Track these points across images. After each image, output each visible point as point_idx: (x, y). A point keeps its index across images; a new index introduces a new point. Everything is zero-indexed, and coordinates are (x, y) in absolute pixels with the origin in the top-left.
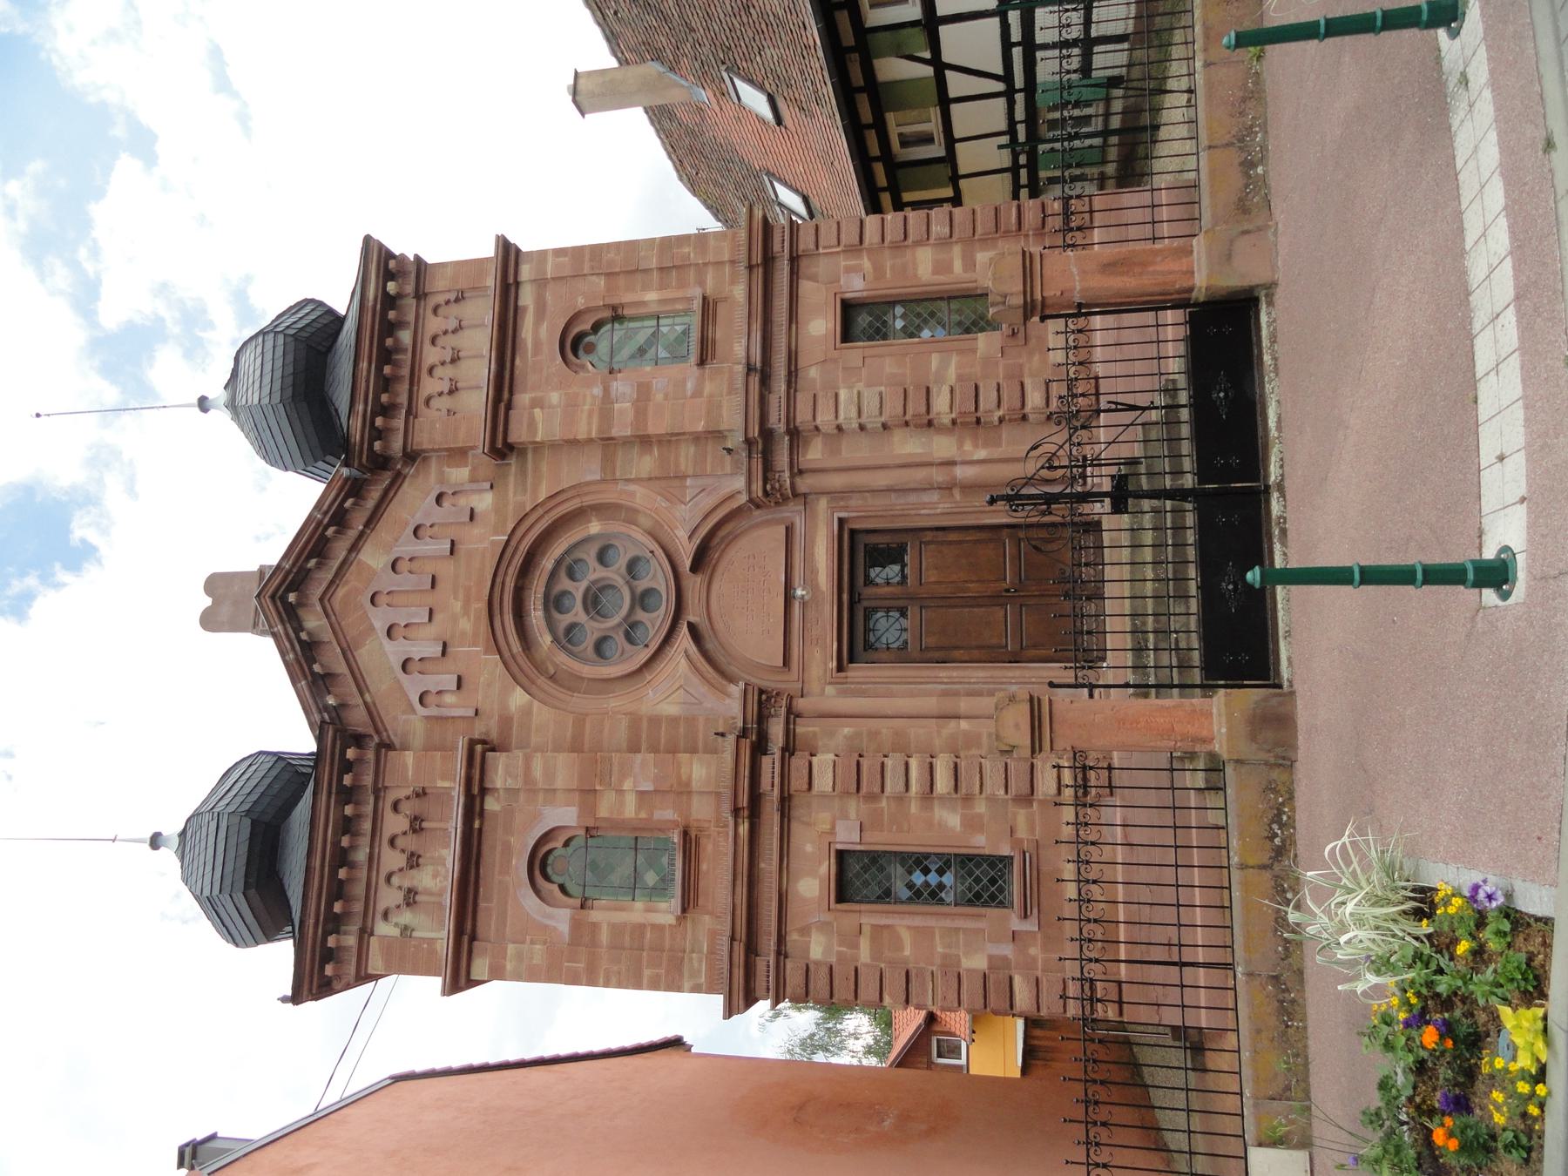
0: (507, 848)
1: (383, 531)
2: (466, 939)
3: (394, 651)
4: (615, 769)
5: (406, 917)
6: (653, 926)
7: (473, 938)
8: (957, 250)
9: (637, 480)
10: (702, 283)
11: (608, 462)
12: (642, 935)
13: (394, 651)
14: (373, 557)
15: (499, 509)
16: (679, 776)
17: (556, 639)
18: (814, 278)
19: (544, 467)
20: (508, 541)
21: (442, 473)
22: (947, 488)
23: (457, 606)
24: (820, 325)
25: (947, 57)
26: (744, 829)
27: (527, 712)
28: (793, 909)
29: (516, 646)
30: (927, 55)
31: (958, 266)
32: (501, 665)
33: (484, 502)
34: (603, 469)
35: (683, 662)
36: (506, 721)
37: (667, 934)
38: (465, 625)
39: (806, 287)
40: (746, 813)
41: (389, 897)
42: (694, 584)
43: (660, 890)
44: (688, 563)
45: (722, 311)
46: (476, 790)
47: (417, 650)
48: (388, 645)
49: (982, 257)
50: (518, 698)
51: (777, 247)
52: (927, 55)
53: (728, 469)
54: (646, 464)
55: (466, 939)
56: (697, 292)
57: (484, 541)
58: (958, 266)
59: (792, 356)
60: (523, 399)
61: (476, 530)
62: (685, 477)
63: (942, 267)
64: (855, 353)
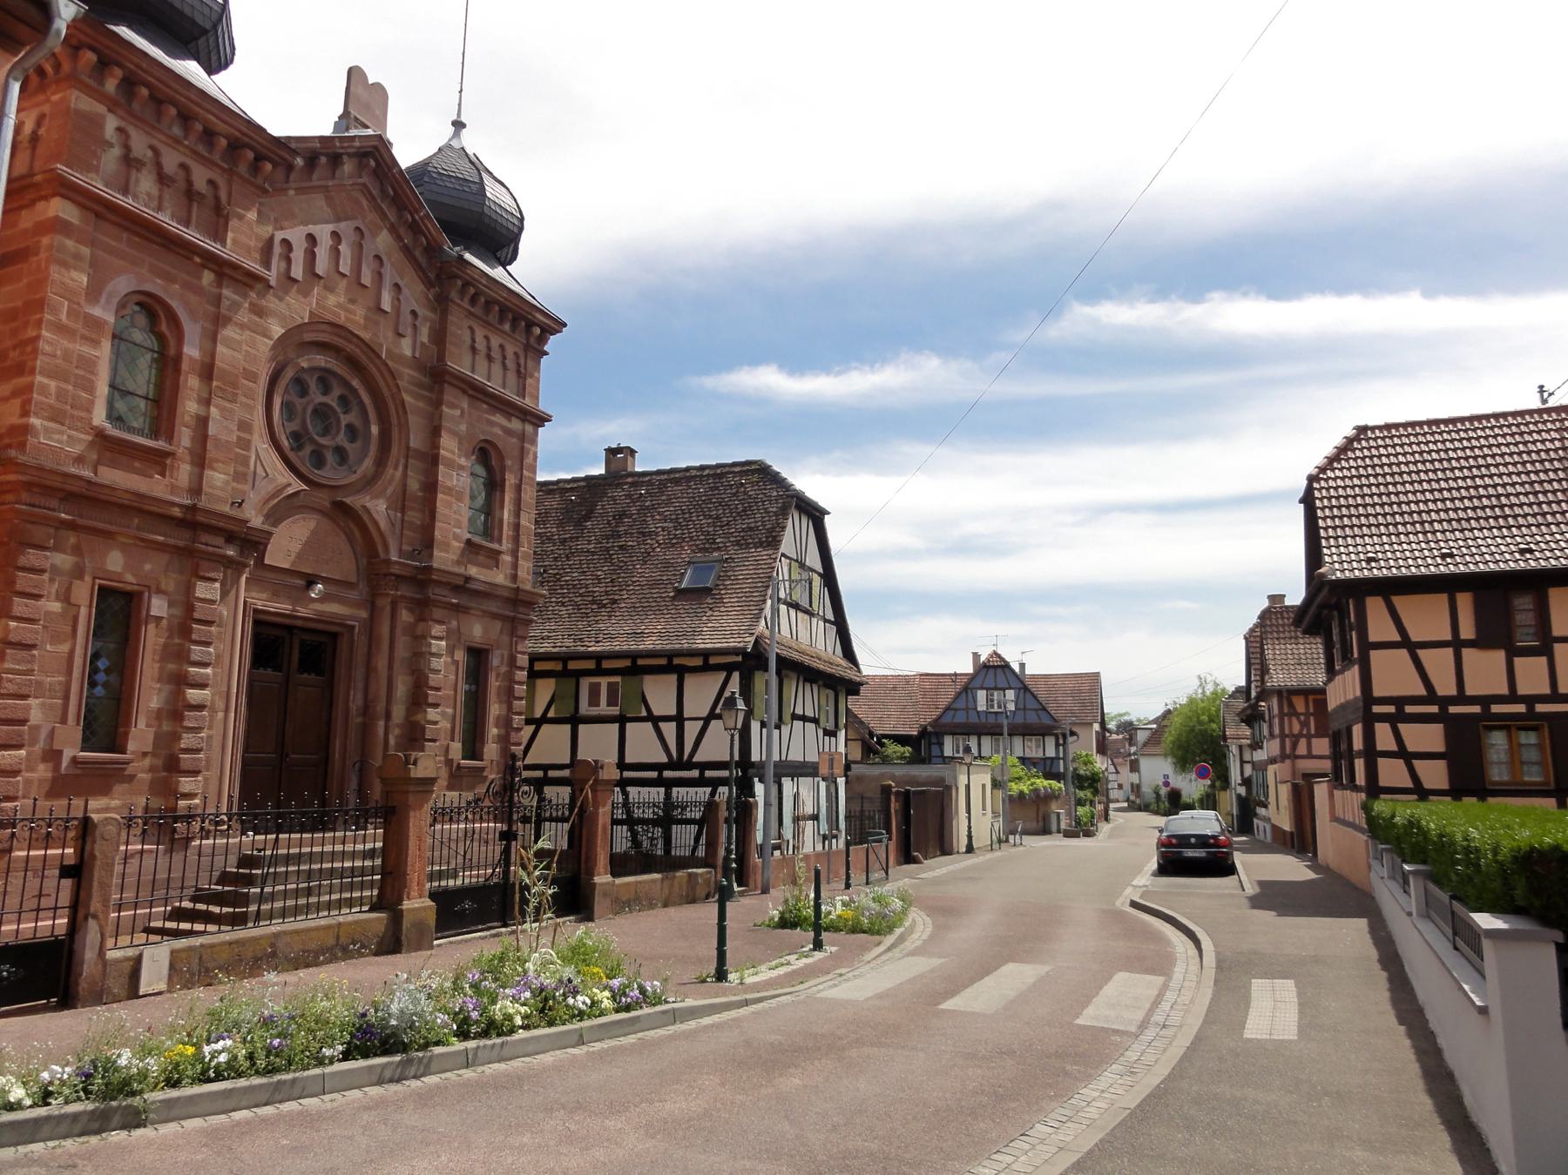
1: (398, 256)
2: (101, 209)
3: (323, 232)
4: (227, 405)
5: (116, 151)
6: (93, 402)
7: (97, 215)
9: (405, 475)
11: (421, 455)
12: (84, 389)
13: (323, 232)
14: (383, 241)
15: (400, 358)
16: (217, 461)
19: (421, 404)
20: (379, 357)
22: (366, 710)
25: (545, 728)
26: (176, 512)
30: (551, 714)
32: (300, 321)
34: (416, 451)
37: (83, 414)
40: (189, 517)
41: (140, 144)
42: (323, 499)
43: (115, 417)
44: (348, 500)
48: (330, 227)
52: (551, 714)
53: (405, 547)
54: (414, 485)
55: (101, 209)
57: (384, 339)
62: (403, 513)
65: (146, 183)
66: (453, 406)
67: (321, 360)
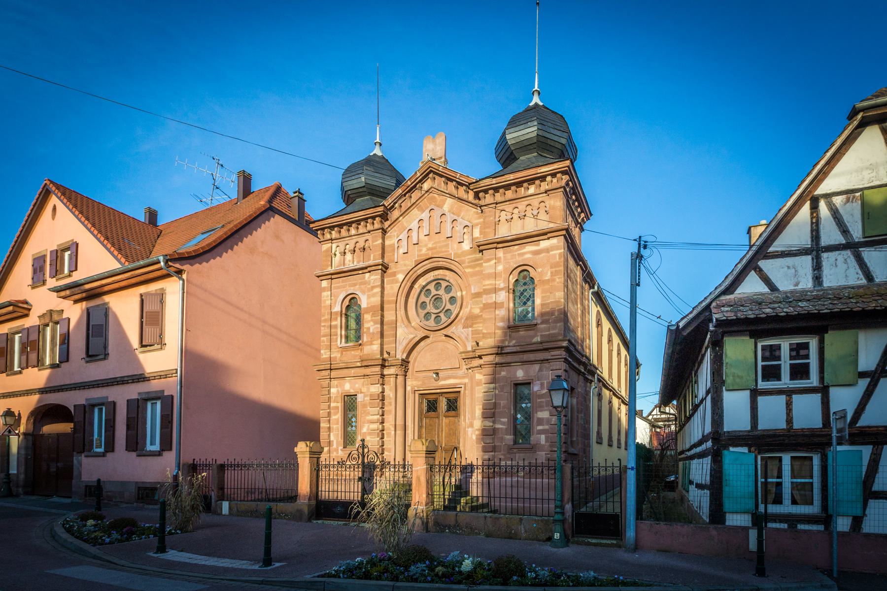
0: (355, 285)
8: (546, 427)
10: (542, 323)
15: (464, 253)
17: (424, 287)
18: (540, 370)
21: (477, 225)
23: (430, 246)
24: (520, 374)
26: (359, 364)
27: (397, 282)
28: (342, 381)
29: (419, 272)
31: (540, 428)
33: (466, 246)
35: (412, 336)
36: (394, 274)
38: (424, 251)
39: (537, 367)
45: (531, 333)
46: (369, 269)
47: (414, 235)
49: (543, 437)
50: (400, 277)
51: (553, 353)
56: (539, 322)
57: (452, 249)
58: (540, 428)
59: (508, 364)
60: (500, 253)
61: (456, 245)
63: (540, 421)
64: (509, 390)
65: (349, 256)
66: (489, 260)
67: (431, 276)
